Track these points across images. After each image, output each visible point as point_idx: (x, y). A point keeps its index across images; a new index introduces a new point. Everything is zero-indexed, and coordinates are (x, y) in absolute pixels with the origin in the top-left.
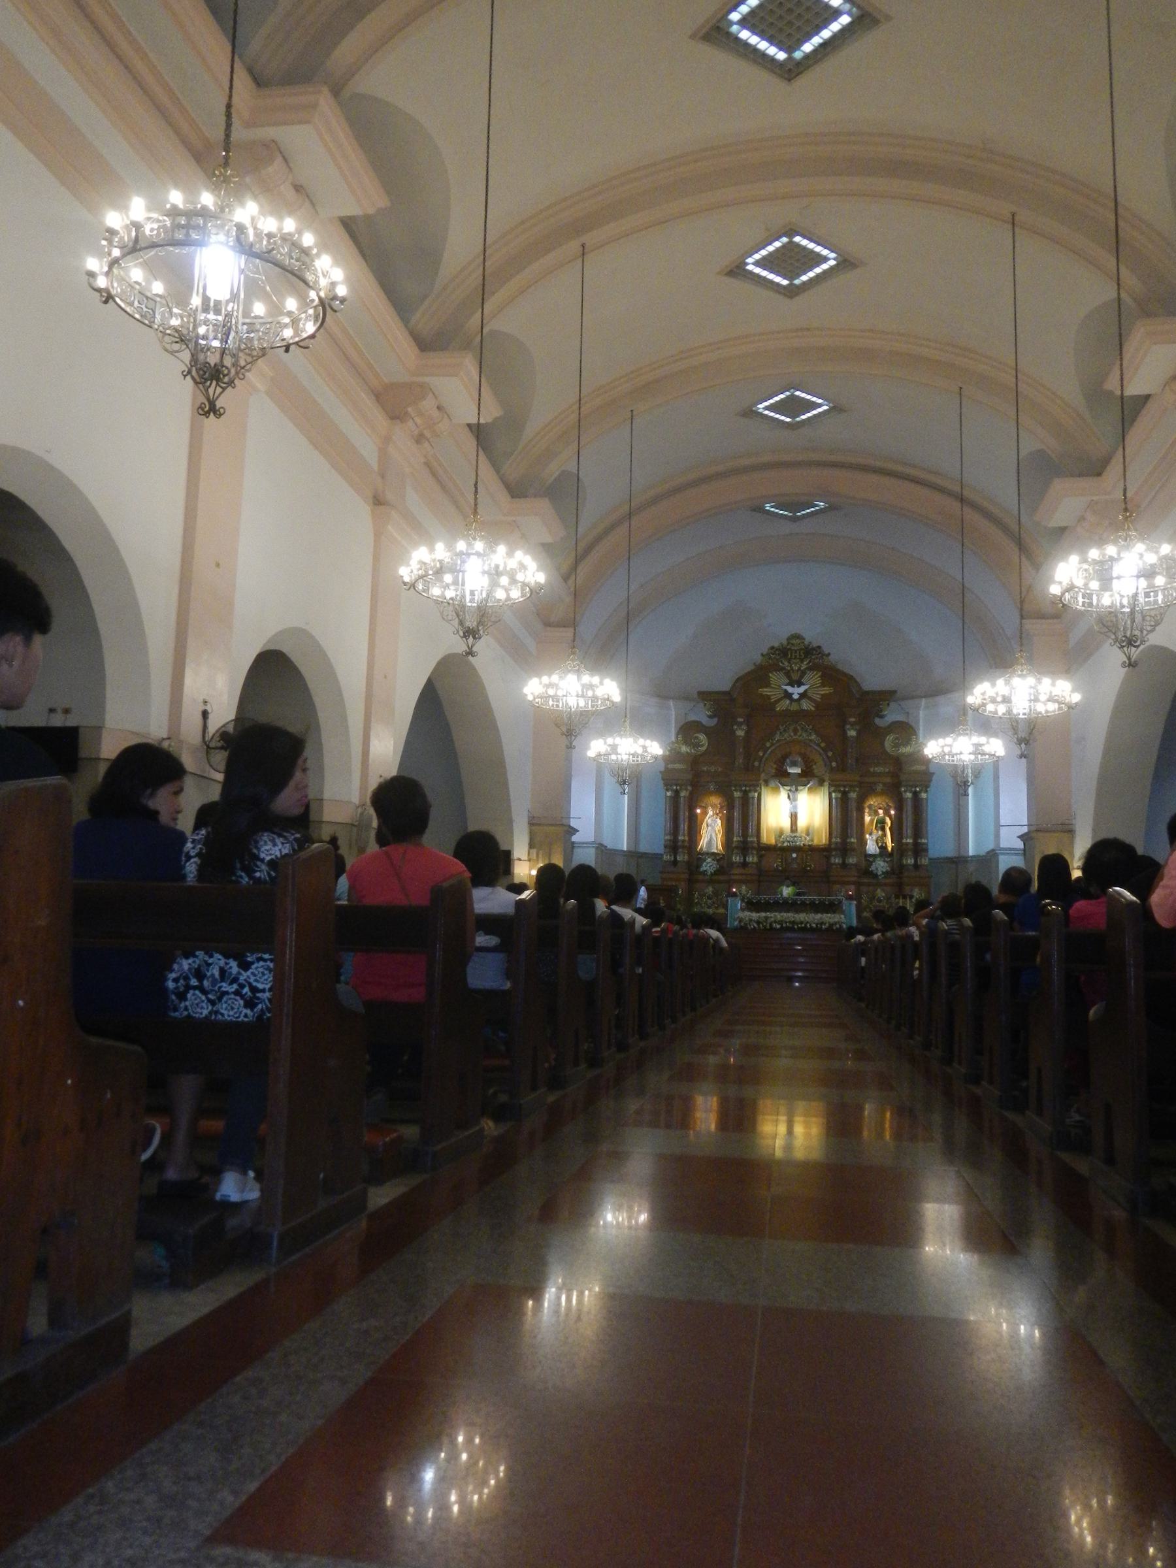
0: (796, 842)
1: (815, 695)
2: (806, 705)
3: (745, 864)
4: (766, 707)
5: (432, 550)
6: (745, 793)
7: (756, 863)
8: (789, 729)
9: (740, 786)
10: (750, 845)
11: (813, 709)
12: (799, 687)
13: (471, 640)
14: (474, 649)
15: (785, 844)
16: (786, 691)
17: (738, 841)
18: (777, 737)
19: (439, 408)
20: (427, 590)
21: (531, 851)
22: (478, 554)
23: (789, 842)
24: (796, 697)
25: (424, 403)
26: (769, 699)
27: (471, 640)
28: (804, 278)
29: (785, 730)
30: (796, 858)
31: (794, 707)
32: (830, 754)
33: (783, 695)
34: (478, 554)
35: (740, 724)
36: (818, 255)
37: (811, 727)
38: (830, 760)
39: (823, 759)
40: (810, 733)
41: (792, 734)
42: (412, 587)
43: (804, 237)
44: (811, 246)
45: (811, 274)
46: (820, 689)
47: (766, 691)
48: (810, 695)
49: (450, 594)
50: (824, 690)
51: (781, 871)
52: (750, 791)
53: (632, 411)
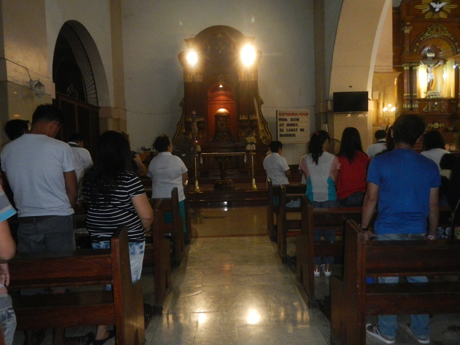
0: (437, 96)
1: (446, 9)
2: (443, 15)
3: (411, 109)
4: (419, 16)
6: (411, 68)
7: (409, 108)
8: (433, 29)
9: (410, 63)
10: (414, 98)
11: (446, 17)
12: (440, 3)
15: (431, 97)
16: (431, 7)
17: (408, 96)
18: (427, 34)
21: (374, 93)
23: (432, 96)
24: (437, 10)
26: (422, 12)
29: (431, 30)
30: (437, 105)
31: (436, 16)
32: (456, 44)
33: (429, 9)
35: (408, 26)
37: (446, 28)
38: (455, 46)
39: (452, 48)
40: (445, 32)
41: (435, 33)
46: (450, 6)
47: (419, 7)
48: (443, 9)
50: (452, 6)
51: (427, 113)
52: (415, 66)
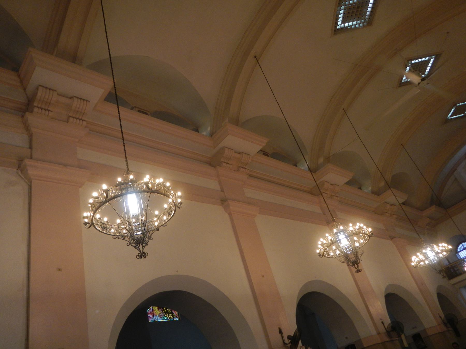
5: (325, 238)
13: (356, 266)
14: (359, 268)
19: (332, 185)
20: (328, 255)
22: (343, 231)
25: (325, 186)
27: (356, 266)
28: (427, 70)
34: (343, 231)
36: (425, 61)
42: (323, 256)
43: (415, 59)
44: (420, 60)
45: (429, 68)
49: (338, 252)
53: (402, 144)
